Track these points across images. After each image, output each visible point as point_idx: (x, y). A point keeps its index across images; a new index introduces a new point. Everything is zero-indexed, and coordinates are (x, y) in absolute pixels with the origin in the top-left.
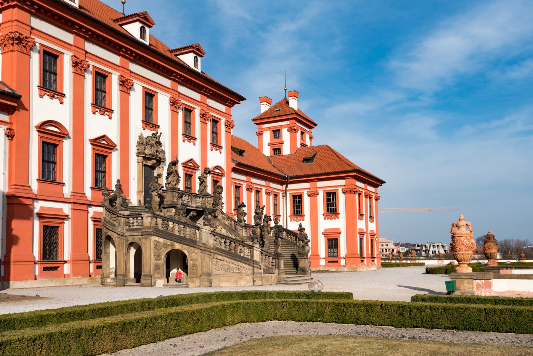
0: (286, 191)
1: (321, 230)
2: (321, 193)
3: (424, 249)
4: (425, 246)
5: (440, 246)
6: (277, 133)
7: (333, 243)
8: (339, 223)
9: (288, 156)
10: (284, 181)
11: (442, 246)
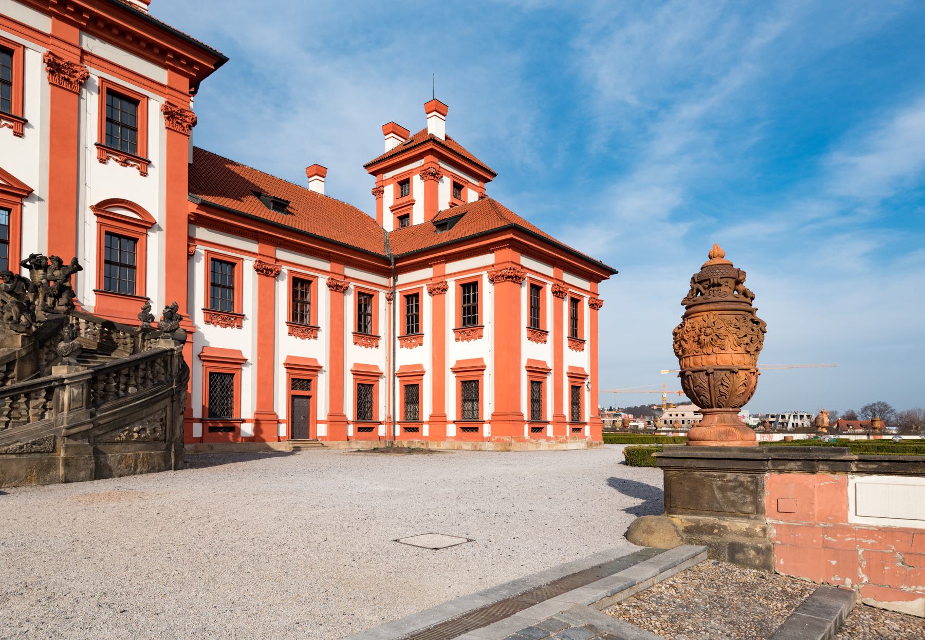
0: (395, 287)
1: (451, 361)
2: (452, 285)
3: (780, 420)
4: (783, 417)
5: (805, 417)
6: (404, 184)
7: (470, 390)
8: (481, 349)
9: (421, 225)
10: (389, 267)
11: (808, 416)
